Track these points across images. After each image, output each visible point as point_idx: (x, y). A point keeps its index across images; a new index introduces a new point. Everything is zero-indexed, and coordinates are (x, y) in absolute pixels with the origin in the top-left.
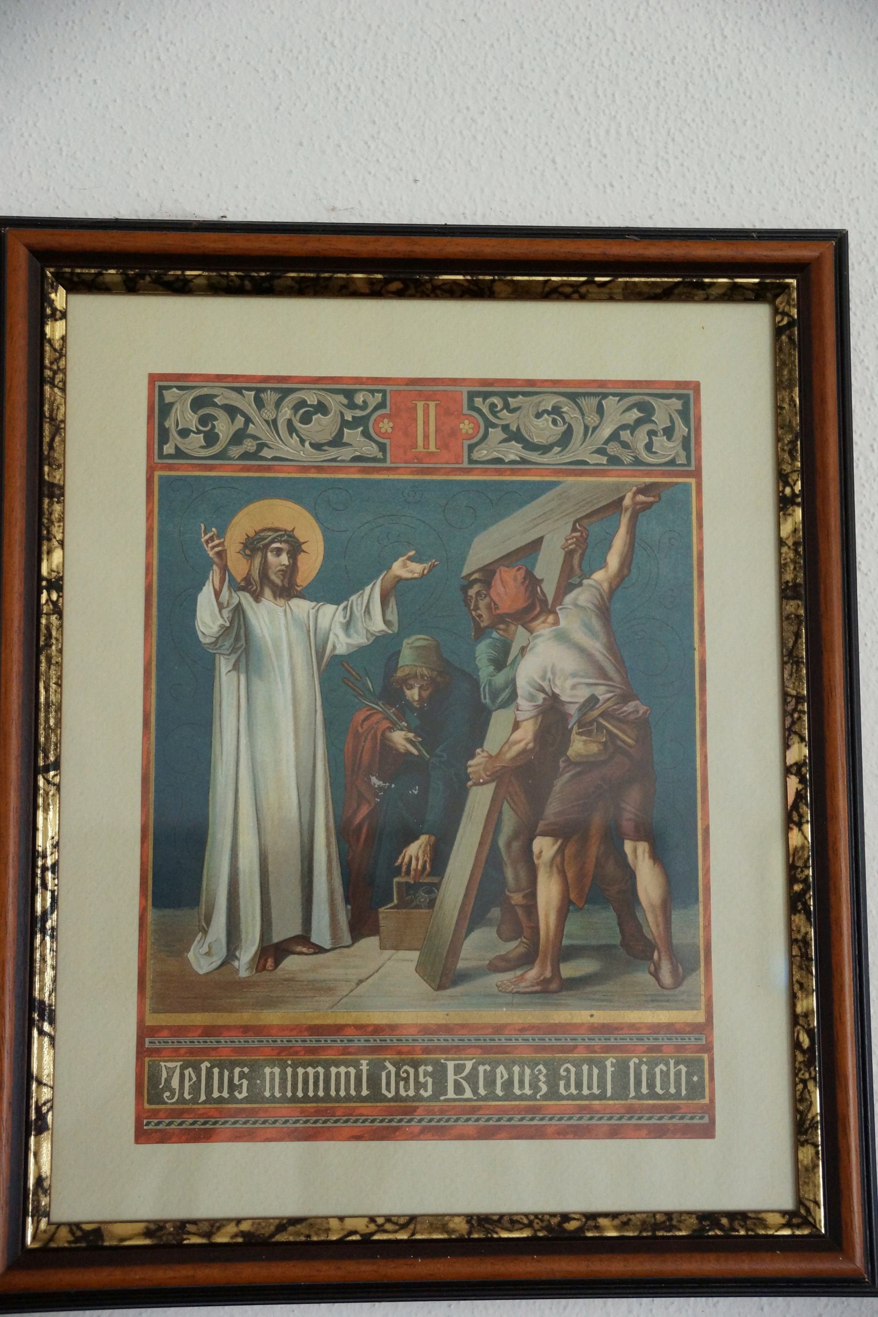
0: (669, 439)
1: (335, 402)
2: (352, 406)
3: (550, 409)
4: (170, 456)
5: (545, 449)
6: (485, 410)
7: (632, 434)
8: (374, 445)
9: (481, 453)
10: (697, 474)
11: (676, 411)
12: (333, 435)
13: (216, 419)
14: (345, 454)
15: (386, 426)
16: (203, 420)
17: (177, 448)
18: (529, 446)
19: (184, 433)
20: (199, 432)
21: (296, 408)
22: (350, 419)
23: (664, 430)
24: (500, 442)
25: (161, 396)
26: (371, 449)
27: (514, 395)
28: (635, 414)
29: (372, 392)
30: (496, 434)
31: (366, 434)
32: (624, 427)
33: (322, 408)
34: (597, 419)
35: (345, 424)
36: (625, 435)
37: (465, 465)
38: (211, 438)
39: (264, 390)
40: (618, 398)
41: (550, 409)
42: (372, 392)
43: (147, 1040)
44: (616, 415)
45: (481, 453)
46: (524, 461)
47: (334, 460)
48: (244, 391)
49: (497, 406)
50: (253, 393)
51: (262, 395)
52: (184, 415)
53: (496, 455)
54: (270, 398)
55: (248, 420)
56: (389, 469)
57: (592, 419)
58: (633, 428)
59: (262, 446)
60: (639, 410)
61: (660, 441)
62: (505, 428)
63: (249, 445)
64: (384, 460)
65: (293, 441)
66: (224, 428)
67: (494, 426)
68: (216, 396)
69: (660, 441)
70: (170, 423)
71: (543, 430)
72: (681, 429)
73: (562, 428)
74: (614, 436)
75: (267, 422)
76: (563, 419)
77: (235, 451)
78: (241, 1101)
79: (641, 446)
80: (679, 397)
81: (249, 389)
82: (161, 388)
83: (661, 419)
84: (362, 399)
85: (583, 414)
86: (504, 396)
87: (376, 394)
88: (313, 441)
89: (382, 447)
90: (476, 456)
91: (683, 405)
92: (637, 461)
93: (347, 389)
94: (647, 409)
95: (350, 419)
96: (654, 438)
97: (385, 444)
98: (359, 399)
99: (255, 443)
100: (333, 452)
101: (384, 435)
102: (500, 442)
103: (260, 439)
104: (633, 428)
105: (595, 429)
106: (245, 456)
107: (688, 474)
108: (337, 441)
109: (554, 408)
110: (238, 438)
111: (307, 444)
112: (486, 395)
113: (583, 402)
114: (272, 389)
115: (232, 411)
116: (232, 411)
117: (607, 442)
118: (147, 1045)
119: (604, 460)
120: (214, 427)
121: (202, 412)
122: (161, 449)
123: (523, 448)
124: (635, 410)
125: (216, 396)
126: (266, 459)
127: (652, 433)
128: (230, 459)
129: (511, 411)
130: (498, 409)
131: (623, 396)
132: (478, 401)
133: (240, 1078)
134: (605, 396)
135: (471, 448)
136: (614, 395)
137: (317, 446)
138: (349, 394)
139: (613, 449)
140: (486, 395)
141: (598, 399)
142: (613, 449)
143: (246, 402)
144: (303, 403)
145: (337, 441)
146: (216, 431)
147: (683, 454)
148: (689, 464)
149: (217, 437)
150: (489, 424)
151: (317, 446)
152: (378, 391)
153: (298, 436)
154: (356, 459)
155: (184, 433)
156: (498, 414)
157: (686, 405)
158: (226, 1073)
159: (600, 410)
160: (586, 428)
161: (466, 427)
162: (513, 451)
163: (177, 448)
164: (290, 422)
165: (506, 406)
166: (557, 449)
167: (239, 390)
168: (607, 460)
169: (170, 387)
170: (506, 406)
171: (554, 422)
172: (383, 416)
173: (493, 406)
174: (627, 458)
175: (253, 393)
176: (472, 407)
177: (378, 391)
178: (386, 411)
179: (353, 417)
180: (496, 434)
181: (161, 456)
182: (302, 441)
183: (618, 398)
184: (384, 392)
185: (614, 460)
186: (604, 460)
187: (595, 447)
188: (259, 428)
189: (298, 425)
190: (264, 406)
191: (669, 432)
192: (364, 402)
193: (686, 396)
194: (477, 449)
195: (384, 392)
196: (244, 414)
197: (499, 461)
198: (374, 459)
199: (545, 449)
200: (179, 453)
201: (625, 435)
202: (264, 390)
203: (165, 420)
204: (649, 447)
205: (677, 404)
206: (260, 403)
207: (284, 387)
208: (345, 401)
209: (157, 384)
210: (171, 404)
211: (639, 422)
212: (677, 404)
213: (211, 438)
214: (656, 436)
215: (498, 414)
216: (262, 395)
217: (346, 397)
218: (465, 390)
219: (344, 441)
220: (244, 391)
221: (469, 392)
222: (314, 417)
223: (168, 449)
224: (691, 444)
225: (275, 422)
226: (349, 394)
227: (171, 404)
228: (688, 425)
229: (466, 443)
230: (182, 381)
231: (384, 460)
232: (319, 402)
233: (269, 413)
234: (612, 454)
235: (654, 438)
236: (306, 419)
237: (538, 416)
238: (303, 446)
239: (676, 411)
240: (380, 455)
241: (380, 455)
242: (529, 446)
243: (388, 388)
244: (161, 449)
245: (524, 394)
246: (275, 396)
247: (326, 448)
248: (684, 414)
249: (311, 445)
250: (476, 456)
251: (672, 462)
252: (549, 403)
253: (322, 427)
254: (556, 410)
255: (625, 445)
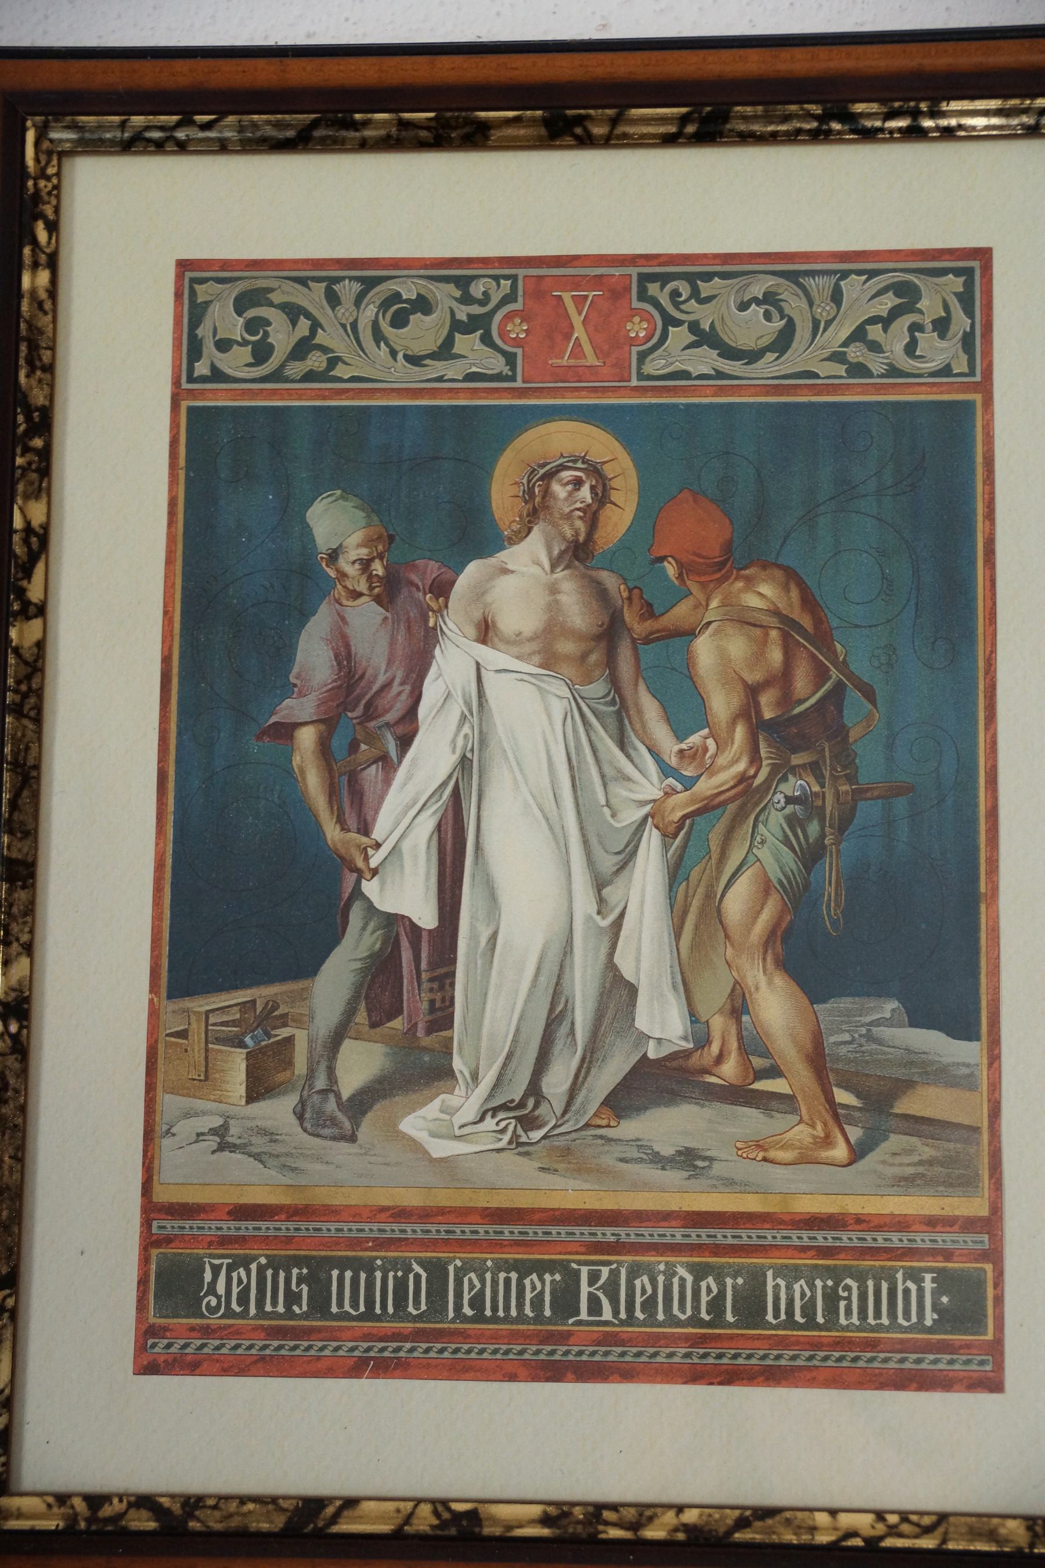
0: (942, 336)
1: (444, 295)
2: (466, 299)
3: (761, 297)
4: (203, 379)
5: (752, 356)
6: (665, 301)
7: (885, 330)
8: (500, 356)
9: (655, 365)
10: (986, 387)
11: (955, 294)
12: (439, 342)
13: (269, 324)
14: (453, 370)
15: (517, 329)
16: (252, 326)
17: (214, 368)
18: (730, 353)
19: (224, 345)
20: (245, 343)
21: (385, 305)
22: (465, 318)
23: (933, 322)
24: (683, 349)
25: (193, 293)
26: (497, 364)
27: (708, 277)
28: (889, 302)
29: (496, 278)
30: (679, 336)
31: (487, 340)
32: (873, 320)
33: (423, 305)
34: (830, 308)
35: (457, 327)
36: (875, 332)
37: (634, 382)
38: (262, 353)
39: (341, 279)
40: (864, 277)
41: (761, 297)
42: (496, 278)
43: (155, 1224)
44: (863, 302)
45: (655, 365)
46: (720, 375)
47: (440, 379)
48: (311, 284)
49: (680, 295)
50: (324, 284)
51: (336, 287)
52: (225, 319)
53: (678, 366)
54: (348, 290)
55: (315, 325)
56: (522, 393)
57: (824, 310)
58: (886, 322)
59: (333, 362)
60: (897, 295)
61: (927, 340)
62: (694, 327)
63: (316, 361)
64: (513, 379)
65: (382, 353)
66: (282, 336)
67: (678, 323)
68: (271, 290)
69: (927, 340)
70: (204, 331)
71: (752, 328)
72: (960, 323)
73: (778, 324)
74: (859, 335)
75: (344, 326)
76: (781, 311)
77: (296, 369)
78: (300, 1317)
79: (899, 347)
80: (957, 272)
81: (318, 280)
82: (193, 281)
83: (929, 306)
84: (483, 289)
85: (811, 304)
86: (691, 279)
87: (502, 282)
88: (409, 353)
89: (510, 359)
90: (649, 368)
91: (965, 284)
92: (893, 371)
93: (460, 273)
94: (908, 294)
95: (465, 318)
96: (917, 334)
97: (515, 354)
98: (477, 290)
99: (324, 358)
100: (437, 368)
101: (517, 342)
102: (683, 349)
103: (333, 351)
104: (886, 322)
105: (829, 323)
106: (310, 376)
107: (974, 387)
108: (445, 351)
109: (764, 294)
110: (302, 349)
111: (400, 356)
112: (664, 279)
113: (810, 282)
114: (351, 278)
115: (293, 312)
116: (293, 312)
117: (845, 344)
118: (154, 1230)
119: (841, 370)
120: (266, 334)
121: (251, 313)
122: (191, 370)
123: (719, 355)
124: (890, 294)
125: (271, 290)
126: (340, 380)
127: (915, 328)
128: (287, 380)
129: (702, 301)
130: (681, 299)
131: (872, 274)
132: (653, 289)
133: (298, 1285)
134: (845, 274)
135: (642, 357)
136: (859, 273)
137: (414, 360)
138: (463, 283)
139: (856, 353)
140: (664, 279)
141: (833, 280)
142: (856, 353)
143: (312, 299)
144: (396, 297)
145: (445, 351)
146: (269, 340)
147: (964, 358)
148: (972, 373)
149: (271, 348)
150: (670, 321)
151: (414, 360)
152: (506, 277)
153: (387, 344)
154: (471, 377)
155: (224, 345)
156: (683, 307)
157: (969, 285)
158: (282, 1275)
159: (837, 297)
160: (816, 324)
161: (637, 329)
162: (704, 361)
163: (214, 368)
164: (375, 325)
165: (695, 294)
166: (770, 356)
167: (303, 281)
168: (847, 371)
169: (202, 281)
170: (695, 294)
171: (768, 316)
172: (509, 317)
173: (675, 294)
174: (876, 364)
175: (324, 284)
176: (643, 296)
177: (506, 277)
178: (518, 306)
179: (469, 315)
180: (679, 336)
181: (191, 379)
182: (393, 354)
183: (864, 277)
184: (514, 278)
185: (859, 370)
186: (841, 370)
187: (826, 353)
188: (330, 337)
189: (385, 326)
190: (339, 303)
191: (942, 326)
192: (485, 293)
193: (971, 270)
194: (651, 357)
195: (514, 278)
196: (308, 315)
197: (685, 375)
198: (498, 377)
199: (752, 356)
200: (217, 375)
201: (875, 332)
202: (341, 279)
203: (197, 326)
204: (910, 349)
205: (957, 283)
206: (333, 299)
207: (370, 273)
208: (458, 294)
209: (189, 275)
210: (207, 304)
211: (895, 313)
212: (957, 283)
213: (262, 353)
214: (923, 332)
215: (683, 307)
216: (336, 287)
217: (457, 287)
218: (634, 271)
219: (455, 350)
220: (311, 284)
221: (639, 274)
222: (412, 317)
223: (202, 368)
224: (978, 343)
225: (354, 325)
226: (463, 283)
227: (207, 304)
228: (970, 313)
229: (635, 350)
230: (224, 270)
231: (513, 379)
232: (418, 294)
233: (346, 311)
234: (855, 360)
235: (917, 334)
236: (400, 321)
237: (743, 307)
238: (395, 360)
239: (955, 294)
240: (506, 370)
241: (506, 370)
242: (730, 353)
243: (521, 272)
244: (191, 370)
245: (724, 276)
246: (357, 287)
247: (427, 362)
248: (966, 299)
249: (406, 357)
250: (649, 368)
251: (946, 371)
252: (758, 290)
253: (423, 332)
254: (769, 299)
255: (875, 347)
